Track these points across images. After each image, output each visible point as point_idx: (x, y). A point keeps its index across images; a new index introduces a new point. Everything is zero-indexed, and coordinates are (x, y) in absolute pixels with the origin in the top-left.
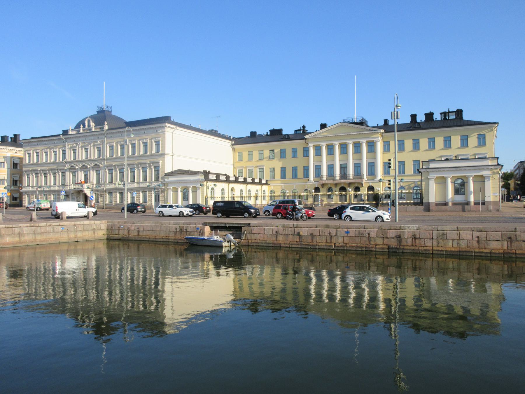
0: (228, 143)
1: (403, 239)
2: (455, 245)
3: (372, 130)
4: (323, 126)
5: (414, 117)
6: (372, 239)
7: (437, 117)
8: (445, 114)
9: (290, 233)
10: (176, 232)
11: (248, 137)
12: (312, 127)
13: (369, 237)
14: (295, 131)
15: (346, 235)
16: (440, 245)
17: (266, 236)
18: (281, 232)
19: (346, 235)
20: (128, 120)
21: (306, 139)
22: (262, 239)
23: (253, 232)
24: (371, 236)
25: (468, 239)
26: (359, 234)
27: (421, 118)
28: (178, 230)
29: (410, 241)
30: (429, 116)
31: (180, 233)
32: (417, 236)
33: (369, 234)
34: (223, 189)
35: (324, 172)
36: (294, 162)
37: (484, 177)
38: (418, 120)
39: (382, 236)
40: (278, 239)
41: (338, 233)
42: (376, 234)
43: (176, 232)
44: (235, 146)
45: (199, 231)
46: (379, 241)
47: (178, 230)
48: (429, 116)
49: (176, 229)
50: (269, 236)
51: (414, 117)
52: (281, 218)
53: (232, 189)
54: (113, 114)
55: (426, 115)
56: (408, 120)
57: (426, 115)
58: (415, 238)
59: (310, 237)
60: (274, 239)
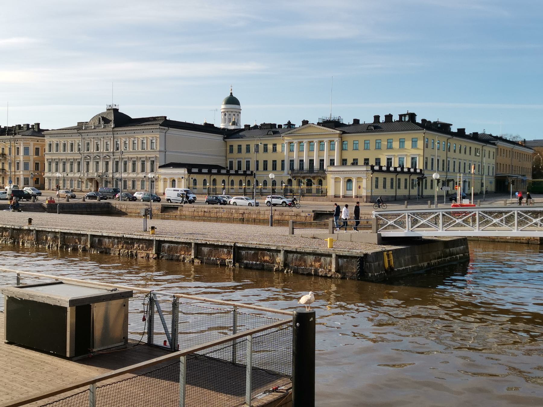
0: (219, 138)
4: (305, 123)
5: (377, 118)
7: (396, 118)
8: (401, 116)
12: (298, 124)
20: (133, 117)
27: (382, 119)
30: (389, 117)
34: (205, 180)
35: (296, 166)
38: (381, 121)
44: (226, 140)
48: (389, 117)
51: (377, 118)
53: (214, 180)
54: (119, 111)
55: (386, 116)
56: (372, 121)
57: (386, 116)
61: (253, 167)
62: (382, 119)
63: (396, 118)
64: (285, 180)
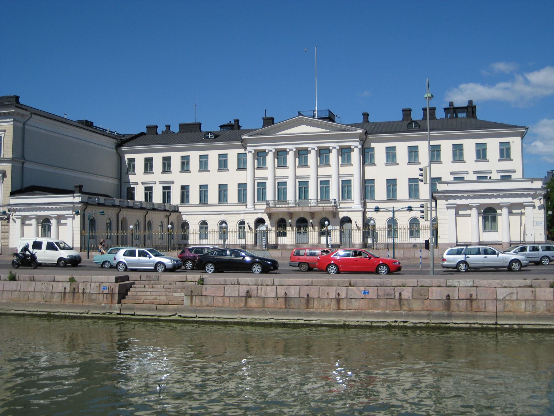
1: (452, 301)
2: (530, 308)
3: (348, 130)
5: (407, 112)
6: (406, 302)
9: (269, 295)
10: (65, 293)
11: (142, 134)
13: (400, 299)
14: (221, 127)
15: (363, 296)
16: (507, 309)
17: (227, 300)
18: (254, 294)
19: (363, 296)
21: (243, 141)
22: (221, 305)
23: (204, 294)
24: (403, 297)
25: (547, 298)
26: (385, 295)
28: (68, 290)
29: (462, 304)
31: (71, 295)
32: (474, 297)
33: (400, 294)
36: (246, 177)
39: (420, 297)
40: (248, 305)
41: (349, 293)
42: (410, 295)
43: (65, 293)
45: (106, 291)
46: (416, 306)
47: (68, 290)
49: (65, 288)
50: (232, 300)
51: (407, 112)
52: (192, 269)
56: (399, 117)
58: (471, 300)
59: (304, 301)
60: (243, 304)
61: (175, 199)
62: (417, 115)
64: (250, 221)
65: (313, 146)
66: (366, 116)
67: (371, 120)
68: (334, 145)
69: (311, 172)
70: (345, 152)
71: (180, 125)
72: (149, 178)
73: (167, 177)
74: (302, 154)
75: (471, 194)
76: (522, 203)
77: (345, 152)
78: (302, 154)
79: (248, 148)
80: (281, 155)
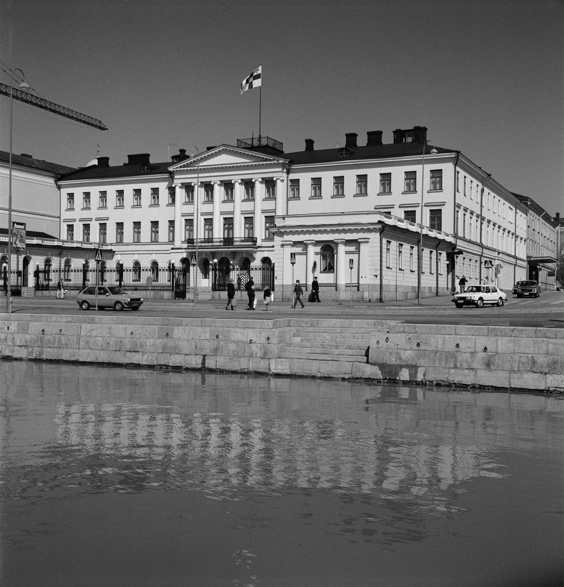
5: (351, 138)
27: (362, 141)
30: (375, 137)
37: (359, 243)
48: (375, 137)
51: (351, 138)
56: (342, 144)
62: (362, 141)
63: (388, 139)
65: (236, 177)
66: (310, 143)
67: (316, 147)
68: (257, 176)
69: (239, 206)
70: (270, 184)
71: (129, 156)
72: (86, 214)
73: (103, 213)
74: (228, 186)
75: (299, 230)
76: (357, 240)
77: (270, 184)
78: (228, 186)
79: (176, 181)
80: (208, 187)
